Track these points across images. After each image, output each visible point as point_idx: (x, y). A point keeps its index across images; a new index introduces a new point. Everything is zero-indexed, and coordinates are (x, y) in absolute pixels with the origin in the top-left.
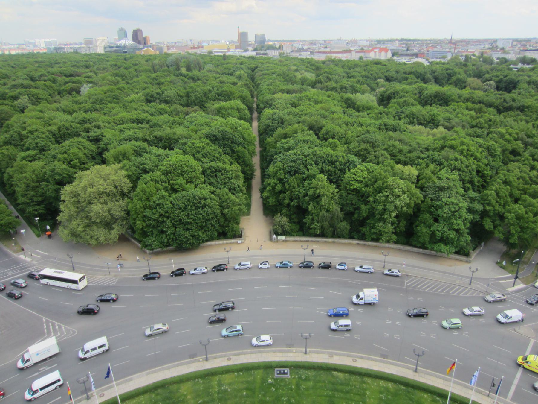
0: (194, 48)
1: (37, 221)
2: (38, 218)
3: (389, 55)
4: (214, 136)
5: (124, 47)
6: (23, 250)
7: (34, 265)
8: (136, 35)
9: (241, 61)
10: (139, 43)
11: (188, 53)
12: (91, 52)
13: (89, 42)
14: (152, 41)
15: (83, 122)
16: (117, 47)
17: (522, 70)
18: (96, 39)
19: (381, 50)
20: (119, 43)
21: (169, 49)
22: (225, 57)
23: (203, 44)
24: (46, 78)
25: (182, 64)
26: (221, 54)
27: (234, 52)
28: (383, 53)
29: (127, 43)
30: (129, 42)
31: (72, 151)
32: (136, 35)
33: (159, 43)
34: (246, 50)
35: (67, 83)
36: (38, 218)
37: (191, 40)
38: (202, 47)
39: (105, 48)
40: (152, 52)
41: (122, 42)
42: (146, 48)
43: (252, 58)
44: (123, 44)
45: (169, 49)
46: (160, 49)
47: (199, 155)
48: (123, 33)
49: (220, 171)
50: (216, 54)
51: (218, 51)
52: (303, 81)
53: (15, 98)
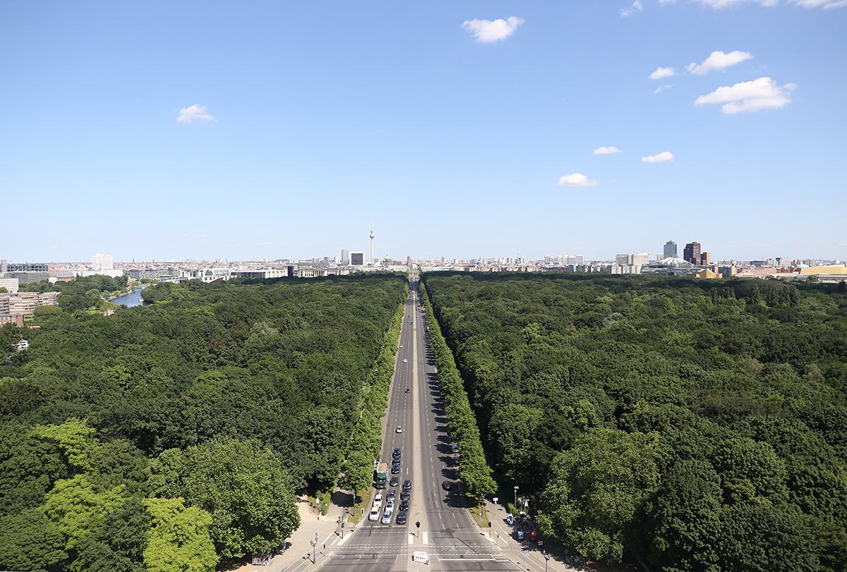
0: (783, 270)
1: (515, 491)
2: (518, 488)
4: (818, 419)
5: (672, 266)
6: (490, 525)
7: (498, 553)
10: (694, 261)
11: (772, 278)
12: (624, 272)
13: (624, 260)
14: (714, 258)
15: (603, 364)
16: (660, 267)
18: (632, 256)
20: (663, 262)
21: (739, 271)
23: (799, 266)
24: (562, 303)
26: (834, 282)
29: (675, 262)
30: (679, 260)
31: (581, 403)
33: (724, 262)
35: (587, 310)
36: (518, 488)
37: (778, 259)
38: (799, 270)
39: (643, 267)
40: (711, 275)
41: (669, 260)
42: (702, 270)
44: (669, 263)
45: (739, 271)
46: (725, 271)
47: (785, 448)
48: (670, 248)
49: (826, 487)
50: (824, 282)
53: (524, 325)
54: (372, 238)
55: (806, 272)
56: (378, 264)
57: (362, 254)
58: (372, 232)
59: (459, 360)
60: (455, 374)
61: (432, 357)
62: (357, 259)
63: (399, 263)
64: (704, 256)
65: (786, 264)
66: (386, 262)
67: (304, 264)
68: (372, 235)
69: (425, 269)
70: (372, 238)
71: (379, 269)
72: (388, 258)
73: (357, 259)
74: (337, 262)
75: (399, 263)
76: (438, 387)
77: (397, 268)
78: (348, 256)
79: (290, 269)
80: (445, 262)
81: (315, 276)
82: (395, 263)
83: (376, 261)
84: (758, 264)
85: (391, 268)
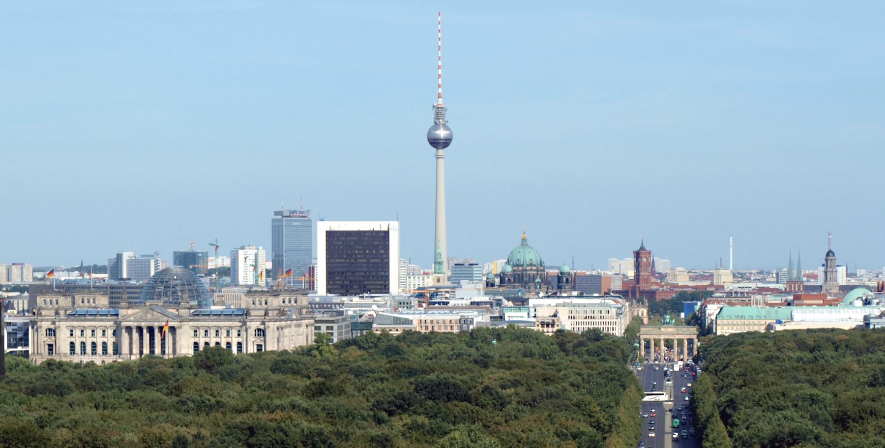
54: (435, 143)
56: (471, 291)
57: (386, 235)
58: (439, 112)
62: (359, 262)
63: (589, 286)
66: (518, 281)
67: (68, 289)
68: (442, 133)
69: (728, 322)
70: (435, 143)
71: (480, 319)
72: (528, 256)
73: (359, 262)
74: (245, 276)
75: (589, 286)
77: (570, 314)
78: (309, 251)
80: (842, 279)
81: (132, 352)
82: (560, 284)
83: (463, 271)
85: (542, 311)
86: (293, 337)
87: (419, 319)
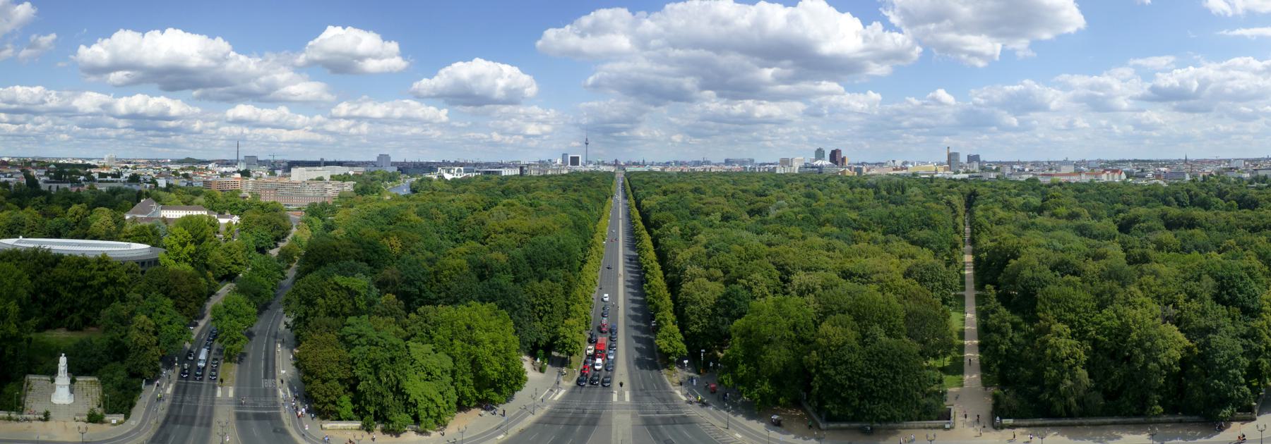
3: (1124, 176)
5: (820, 168)
8: (834, 156)
9: (952, 184)
10: (836, 163)
13: (785, 162)
17: (1257, 188)
19: (1114, 171)
22: (932, 179)
25: (883, 187)
27: (941, 173)
28: (1116, 175)
30: (826, 162)
32: (834, 156)
34: (958, 172)
40: (849, 173)
41: (819, 163)
43: (964, 180)
48: (820, 154)
51: (924, 170)
52: (1026, 207)
53: (707, 214)
55: (911, 169)
59: (656, 244)
60: (651, 255)
61: (634, 241)
64: (844, 160)
65: (899, 163)
73: (575, 161)
76: (636, 264)
79: (521, 168)
84: (881, 164)
86: (566, 172)
87: (583, 169)
